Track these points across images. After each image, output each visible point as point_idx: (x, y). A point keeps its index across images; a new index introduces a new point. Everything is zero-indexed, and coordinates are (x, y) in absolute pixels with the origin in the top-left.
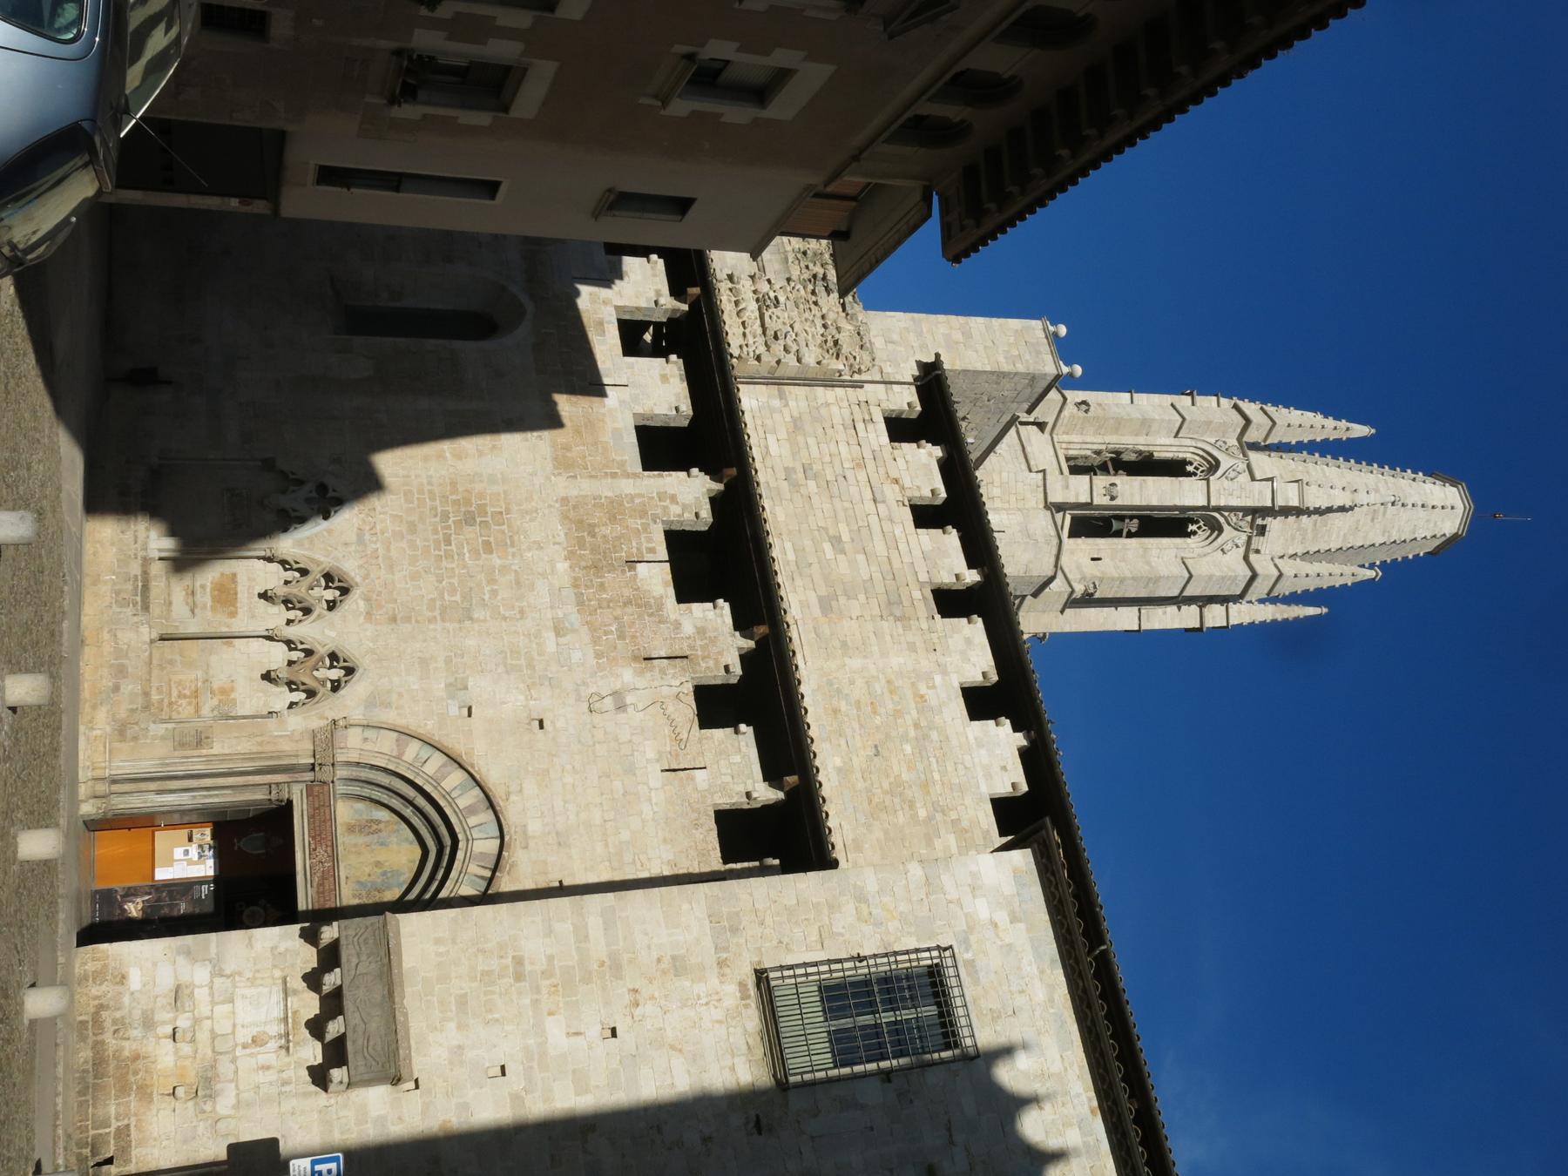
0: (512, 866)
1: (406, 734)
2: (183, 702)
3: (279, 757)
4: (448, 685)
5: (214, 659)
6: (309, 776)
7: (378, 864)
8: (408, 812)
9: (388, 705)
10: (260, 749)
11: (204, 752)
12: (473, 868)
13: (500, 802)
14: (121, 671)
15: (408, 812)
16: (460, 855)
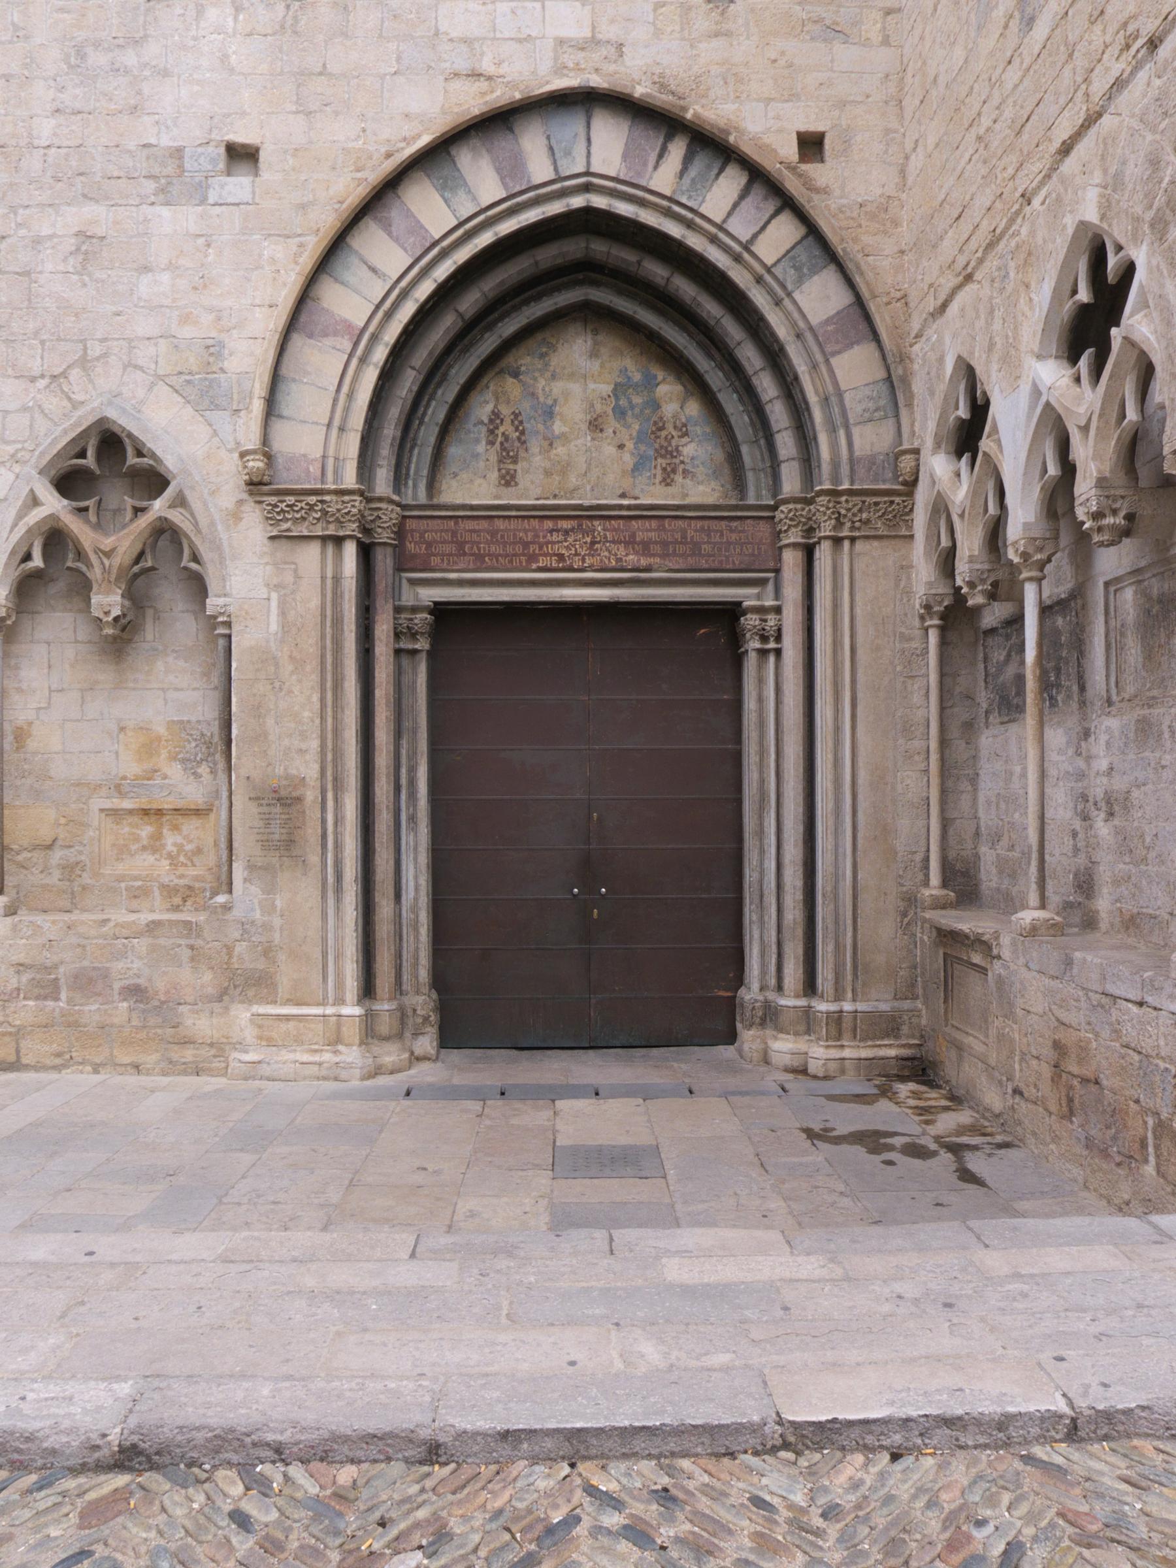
0: (663, 87)
1: (300, 315)
2: (171, 840)
3: (338, 622)
4: (165, 195)
5: (58, 769)
6: (384, 562)
7: (595, 425)
8: (488, 344)
9: (214, 351)
10: (312, 666)
11: (311, 795)
12: (664, 177)
13: (500, 96)
14: (88, 982)
15: (488, 344)
16: (624, 209)
